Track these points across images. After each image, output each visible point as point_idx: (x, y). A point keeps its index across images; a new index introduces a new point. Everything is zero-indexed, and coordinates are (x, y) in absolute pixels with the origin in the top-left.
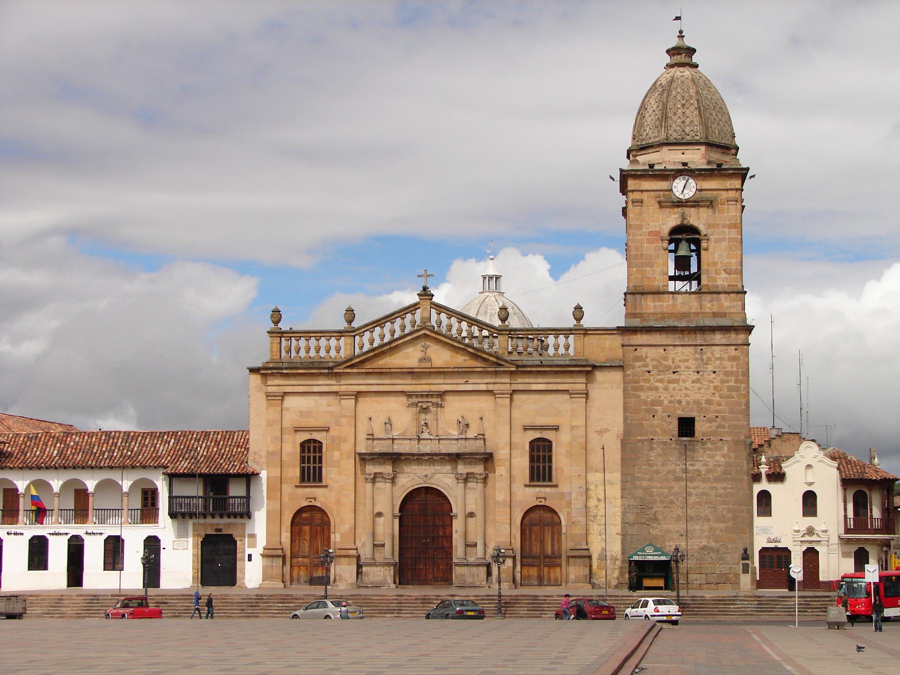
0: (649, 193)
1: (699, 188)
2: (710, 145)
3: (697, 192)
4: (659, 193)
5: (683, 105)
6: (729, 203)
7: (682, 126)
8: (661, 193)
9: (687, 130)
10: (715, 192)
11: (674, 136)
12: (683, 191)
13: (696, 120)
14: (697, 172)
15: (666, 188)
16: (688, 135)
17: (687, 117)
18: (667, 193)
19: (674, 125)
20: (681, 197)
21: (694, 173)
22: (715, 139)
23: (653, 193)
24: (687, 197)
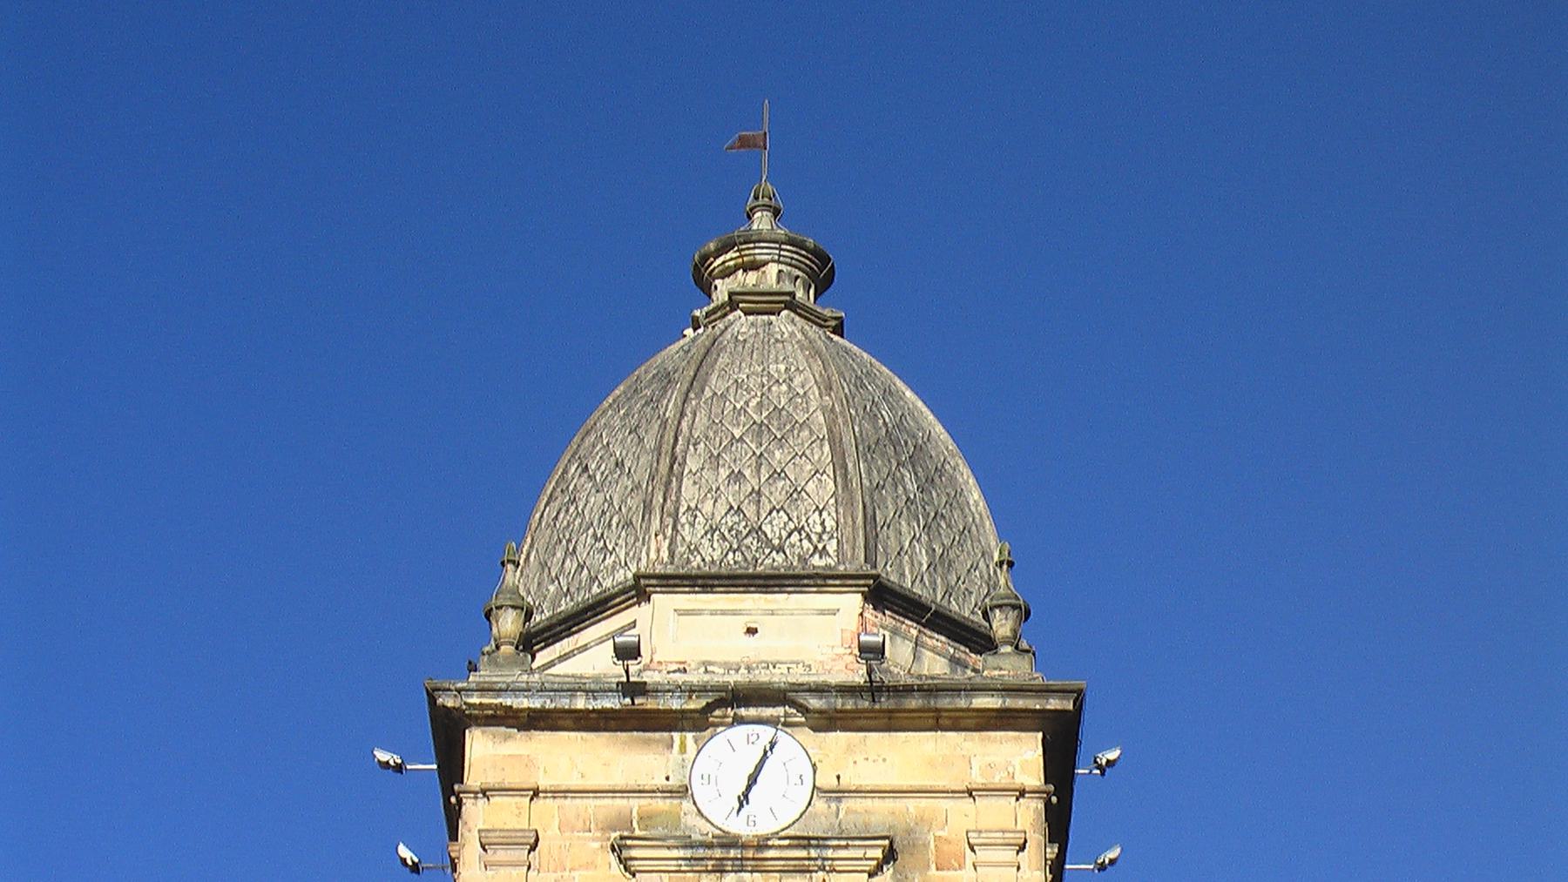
0: (569, 804)
1: (827, 780)
2: (881, 596)
3: (820, 805)
4: (620, 803)
5: (759, 429)
6: (982, 854)
7: (750, 510)
8: (635, 805)
9: (774, 528)
10: (913, 805)
11: (711, 554)
12: (744, 799)
13: (823, 489)
14: (814, 703)
15: (660, 782)
16: (780, 549)
17: (777, 475)
18: (661, 804)
19: (707, 507)
20: (738, 826)
21: (804, 710)
22: (908, 577)
23: (591, 803)
24: (766, 827)
